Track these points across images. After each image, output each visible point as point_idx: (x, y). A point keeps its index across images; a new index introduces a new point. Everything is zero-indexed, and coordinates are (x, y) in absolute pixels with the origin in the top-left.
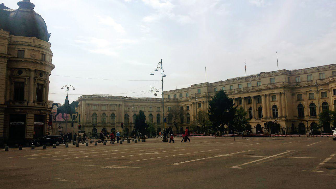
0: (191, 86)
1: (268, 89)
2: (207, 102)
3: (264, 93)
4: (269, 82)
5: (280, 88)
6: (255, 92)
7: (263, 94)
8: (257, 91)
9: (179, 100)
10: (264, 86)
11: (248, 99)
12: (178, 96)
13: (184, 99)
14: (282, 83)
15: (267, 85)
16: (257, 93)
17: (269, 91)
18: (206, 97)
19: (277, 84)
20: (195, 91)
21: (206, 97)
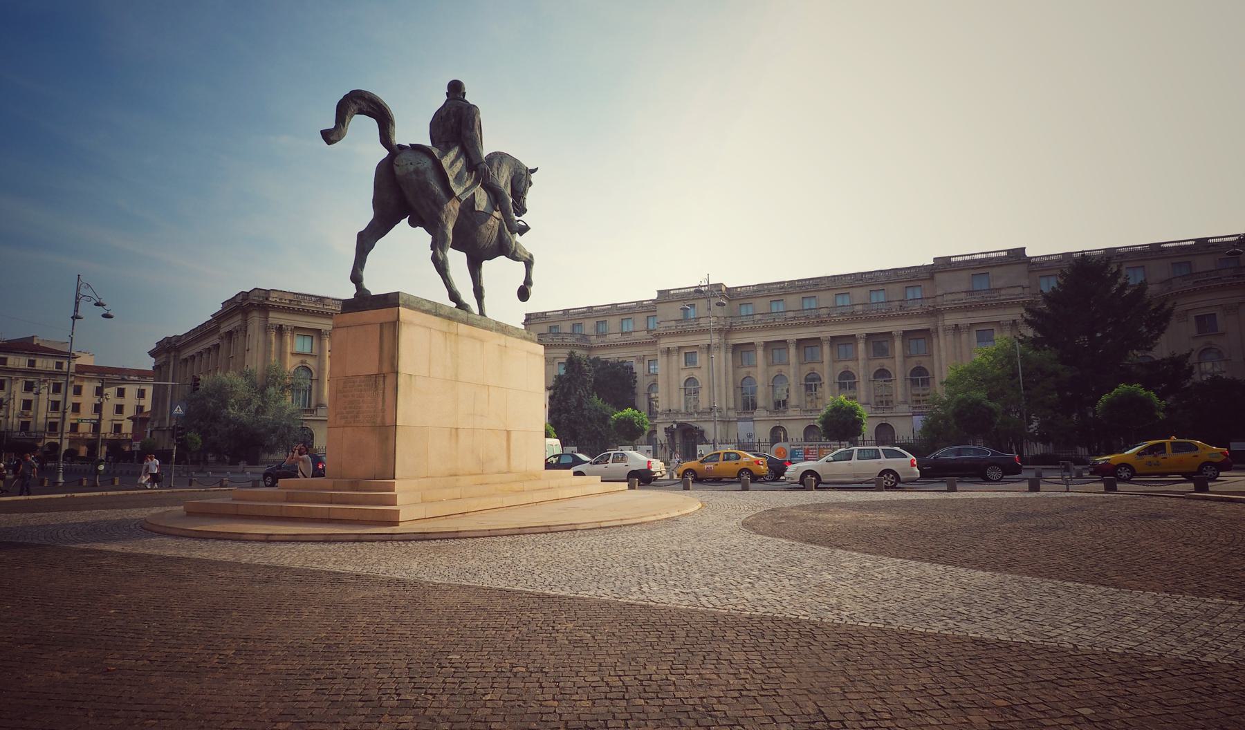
0: (655, 296)
1: (967, 308)
2: (723, 350)
3: (950, 320)
4: (965, 287)
5: (1012, 305)
6: (910, 316)
7: (947, 323)
8: (918, 315)
9: (594, 340)
10: (950, 297)
11: (878, 343)
12: (589, 327)
13: (614, 338)
14: (1019, 290)
15: (963, 296)
16: (917, 321)
17: (970, 314)
18: (720, 331)
19: (1003, 292)
20: (674, 311)
21: (720, 331)
